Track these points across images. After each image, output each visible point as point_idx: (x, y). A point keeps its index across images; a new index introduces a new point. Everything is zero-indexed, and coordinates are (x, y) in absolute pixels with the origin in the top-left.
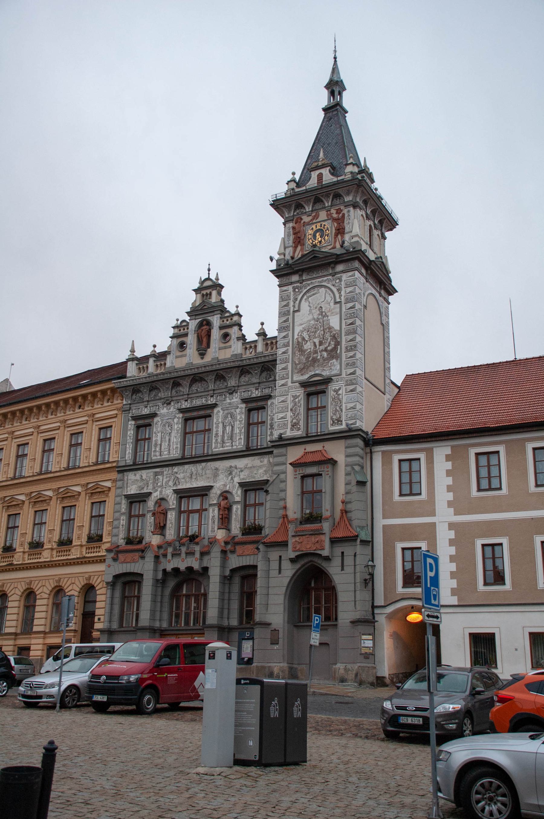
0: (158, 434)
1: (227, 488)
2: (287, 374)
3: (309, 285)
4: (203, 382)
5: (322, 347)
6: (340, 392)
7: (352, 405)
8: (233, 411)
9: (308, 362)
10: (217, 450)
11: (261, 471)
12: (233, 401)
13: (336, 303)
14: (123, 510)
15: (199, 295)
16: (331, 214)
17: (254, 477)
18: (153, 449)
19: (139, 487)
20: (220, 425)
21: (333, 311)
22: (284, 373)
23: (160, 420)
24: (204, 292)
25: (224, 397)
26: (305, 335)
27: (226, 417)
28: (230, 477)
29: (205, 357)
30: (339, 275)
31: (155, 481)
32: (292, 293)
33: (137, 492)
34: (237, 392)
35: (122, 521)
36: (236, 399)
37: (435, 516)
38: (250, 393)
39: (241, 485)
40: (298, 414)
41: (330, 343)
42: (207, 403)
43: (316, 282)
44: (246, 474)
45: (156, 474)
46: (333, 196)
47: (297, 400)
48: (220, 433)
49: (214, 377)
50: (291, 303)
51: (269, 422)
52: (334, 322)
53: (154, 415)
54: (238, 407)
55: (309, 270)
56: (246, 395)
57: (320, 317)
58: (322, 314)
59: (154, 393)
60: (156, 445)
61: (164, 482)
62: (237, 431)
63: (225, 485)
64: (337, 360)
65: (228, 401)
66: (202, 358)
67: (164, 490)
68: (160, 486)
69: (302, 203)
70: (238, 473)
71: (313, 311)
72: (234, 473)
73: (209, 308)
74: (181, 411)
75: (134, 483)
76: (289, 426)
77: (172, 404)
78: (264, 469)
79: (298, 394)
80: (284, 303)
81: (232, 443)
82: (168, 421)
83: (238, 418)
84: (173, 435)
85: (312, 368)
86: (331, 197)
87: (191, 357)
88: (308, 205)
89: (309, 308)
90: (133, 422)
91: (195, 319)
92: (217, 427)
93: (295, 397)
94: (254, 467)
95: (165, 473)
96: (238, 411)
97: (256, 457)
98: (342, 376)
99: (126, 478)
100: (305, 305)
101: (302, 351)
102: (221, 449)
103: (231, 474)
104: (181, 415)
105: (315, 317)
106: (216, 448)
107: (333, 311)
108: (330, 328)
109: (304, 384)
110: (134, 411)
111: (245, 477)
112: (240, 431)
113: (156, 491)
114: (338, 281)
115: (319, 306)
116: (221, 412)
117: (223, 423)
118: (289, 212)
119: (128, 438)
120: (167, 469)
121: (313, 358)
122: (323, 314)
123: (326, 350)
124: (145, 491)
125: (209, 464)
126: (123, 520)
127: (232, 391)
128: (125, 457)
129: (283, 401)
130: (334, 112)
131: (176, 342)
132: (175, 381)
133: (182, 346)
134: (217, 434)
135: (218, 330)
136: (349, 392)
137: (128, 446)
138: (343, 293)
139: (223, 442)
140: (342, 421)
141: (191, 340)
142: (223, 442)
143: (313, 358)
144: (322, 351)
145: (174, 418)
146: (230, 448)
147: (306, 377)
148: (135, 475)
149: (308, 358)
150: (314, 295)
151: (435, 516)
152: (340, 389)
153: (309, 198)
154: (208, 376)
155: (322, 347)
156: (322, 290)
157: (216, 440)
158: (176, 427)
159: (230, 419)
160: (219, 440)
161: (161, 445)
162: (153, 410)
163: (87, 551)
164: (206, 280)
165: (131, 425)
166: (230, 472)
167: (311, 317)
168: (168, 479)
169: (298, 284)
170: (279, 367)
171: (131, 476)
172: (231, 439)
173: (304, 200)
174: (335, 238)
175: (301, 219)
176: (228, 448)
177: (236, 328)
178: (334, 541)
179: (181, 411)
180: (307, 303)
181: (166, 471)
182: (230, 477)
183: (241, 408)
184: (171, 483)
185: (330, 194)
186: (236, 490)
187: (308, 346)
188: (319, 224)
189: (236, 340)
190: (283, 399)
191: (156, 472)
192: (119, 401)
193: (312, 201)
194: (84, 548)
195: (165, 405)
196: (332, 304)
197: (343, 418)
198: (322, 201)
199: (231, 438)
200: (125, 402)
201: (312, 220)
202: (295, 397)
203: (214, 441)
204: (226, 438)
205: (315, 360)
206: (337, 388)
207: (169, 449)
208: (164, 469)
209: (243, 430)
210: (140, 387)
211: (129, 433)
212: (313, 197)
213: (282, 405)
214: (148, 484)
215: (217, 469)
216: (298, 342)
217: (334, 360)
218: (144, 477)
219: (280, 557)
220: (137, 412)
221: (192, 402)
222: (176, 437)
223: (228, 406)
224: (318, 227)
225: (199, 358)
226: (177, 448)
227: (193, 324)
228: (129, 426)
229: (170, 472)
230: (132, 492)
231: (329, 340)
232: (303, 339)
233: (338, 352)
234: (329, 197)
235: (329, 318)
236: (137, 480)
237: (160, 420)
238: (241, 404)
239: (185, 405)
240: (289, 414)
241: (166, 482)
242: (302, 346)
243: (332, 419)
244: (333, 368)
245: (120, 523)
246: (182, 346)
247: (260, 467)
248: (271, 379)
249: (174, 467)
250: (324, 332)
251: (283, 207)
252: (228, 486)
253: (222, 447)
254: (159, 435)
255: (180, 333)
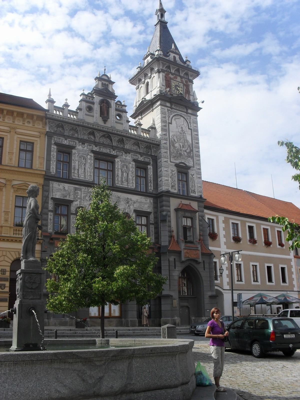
0: (76, 162)
1: (126, 211)
2: (168, 156)
3: (175, 112)
4: (107, 139)
5: (184, 149)
6: (194, 176)
7: (200, 185)
8: (127, 164)
9: (178, 154)
10: (119, 185)
11: (146, 206)
12: (127, 158)
13: (189, 129)
14: (50, 208)
15: (100, 83)
16: (183, 81)
17: (142, 209)
18: (73, 171)
19: (63, 195)
20: (119, 170)
21: (188, 132)
22: (165, 154)
23: (77, 153)
24: (104, 82)
25: (121, 153)
26: (175, 138)
27: (123, 166)
28: (128, 205)
29: (107, 123)
30: (190, 115)
31: (75, 194)
32: (167, 112)
33: (62, 198)
34: (129, 153)
35: (49, 216)
36: (129, 157)
37: (220, 248)
38: (137, 157)
39: (135, 211)
40: (174, 181)
41: (187, 148)
42: (110, 153)
43: (179, 113)
44: (138, 205)
45: (76, 189)
46: (185, 73)
47: (173, 173)
48: (120, 175)
49: (117, 139)
50: (167, 118)
51: (149, 179)
52: (189, 138)
53: (73, 148)
54: (130, 163)
55: (177, 104)
56: (135, 157)
57: (182, 132)
58: (183, 131)
59: (72, 132)
60: (74, 168)
61: (82, 196)
62: (130, 177)
63: (125, 209)
64: (191, 158)
65: (125, 157)
66: (105, 123)
67: (82, 201)
68: (79, 198)
69: (171, 67)
70: (133, 203)
71: (178, 127)
72: (130, 203)
73: (103, 93)
74: (93, 152)
75: (59, 190)
76: (170, 186)
77: (86, 145)
78: (148, 205)
79: (174, 170)
80: (164, 116)
81: (128, 184)
82: (83, 155)
83: (131, 170)
84: (87, 166)
85: (180, 158)
86: (184, 73)
87: (95, 118)
88: (173, 70)
89: (176, 125)
90: (55, 147)
91: (99, 96)
92: (118, 171)
93: (173, 171)
94: (142, 202)
95: (83, 190)
96: (130, 165)
97: (143, 197)
98: (194, 168)
99: (51, 185)
100: (174, 122)
101: (173, 146)
102: (121, 185)
103: (128, 203)
104: (92, 155)
105: (180, 131)
106: (118, 184)
107: (188, 132)
108: (187, 141)
109: (177, 165)
110: (56, 139)
111: (137, 206)
112: (133, 178)
113: (77, 201)
114: (189, 118)
115: (181, 126)
116: (120, 163)
117: (122, 170)
118: (163, 67)
119: (52, 157)
120: (84, 188)
121: (180, 153)
122: (183, 132)
123: (186, 151)
124: (67, 198)
125: (114, 192)
126: (51, 215)
127: (127, 151)
128: (50, 170)
129: (166, 171)
130: (163, 25)
131: (84, 104)
132: (92, 130)
133: (90, 109)
134: (118, 175)
135: (115, 110)
136: (198, 178)
137: (51, 162)
138: (192, 125)
139: (122, 182)
140: (195, 192)
141: (97, 107)
142: (122, 182)
143: (180, 153)
144: (184, 151)
145: (88, 155)
146: (127, 187)
147: (177, 162)
148: (59, 185)
149: (177, 152)
150: (178, 119)
151: (220, 248)
152: (193, 175)
153: (175, 66)
154: (115, 137)
155: (184, 149)
156: (182, 118)
157: (118, 179)
158: (89, 161)
159: (125, 168)
160: (120, 179)
161: (78, 170)
162: (72, 143)
163: (15, 232)
164: (103, 75)
165: (53, 148)
166: (128, 201)
167: (177, 130)
168: (85, 195)
169: (170, 109)
170: (163, 150)
171: (55, 185)
172: (127, 181)
173: (173, 66)
174: (185, 94)
175: (169, 74)
176: (125, 185)
177: (125, 114)
178: (203, 254)
179: (93, 152)
180: (175, 122)
181: (83, 188)
182: (128, 205)
183: (133, 165)
184: (87, 198)
185: (185, 71)
186: (132, 213)
187: (177, 145)
188: (177, 82)
189: (126, 121)
190: (166, 169)
191: (76, 188)
192: (41, 127)
193: (176, 69)
194: (12, 230)
195: (81, 144)
196: (187, 128)
197: (196, 191)
198: (179, 72)
199: (127, 181)
200: (48, 130)
201: (174, 78)
202: (173, 171)
203: (116, 179)
204: (124, 180)
205: (181, 154)
206: (193, 174)
207: (85, 175)
208: (82, 187)
209: (134, 178)
210: (65, 125)
211: (52, 154)
212: (177, 68)
213: (166, 172)
214: (69, 194)
215: (119, 197)
216: (172, 141)
217: (190, 159)
218: (66, 188)
219: (175, 259)
220: (59, 141)
221: (100, 149)
222: (89, 168)
223: (124, 160)
224: (177, 84)
225: (103, 122)
226: (90, 175)
227: (97, 99)
228: (52, 148)
229: (86, 190)
230: (57, 197)
231: (187, 147)
232: (174, 140)
233: (192, 155)
234: (183, 72)
235: (186, 135)
236: (60, 189)
237: (77, 153)
238: (132, 162)
239: (96, 149)
240: (170, 179)
241: (84, 197)
242: (174, 144)
243: (191, 189)
244: (189, 163)
245: (48, 216)
246: (90, 109)
247: (146, 203)
248: (149, 154)
249: (89, 188)
250: (185, 141)
251: (162, 62)
252: (127, 210)
253: (122, 185)
254: (77, 162)
255: (87, 100)
